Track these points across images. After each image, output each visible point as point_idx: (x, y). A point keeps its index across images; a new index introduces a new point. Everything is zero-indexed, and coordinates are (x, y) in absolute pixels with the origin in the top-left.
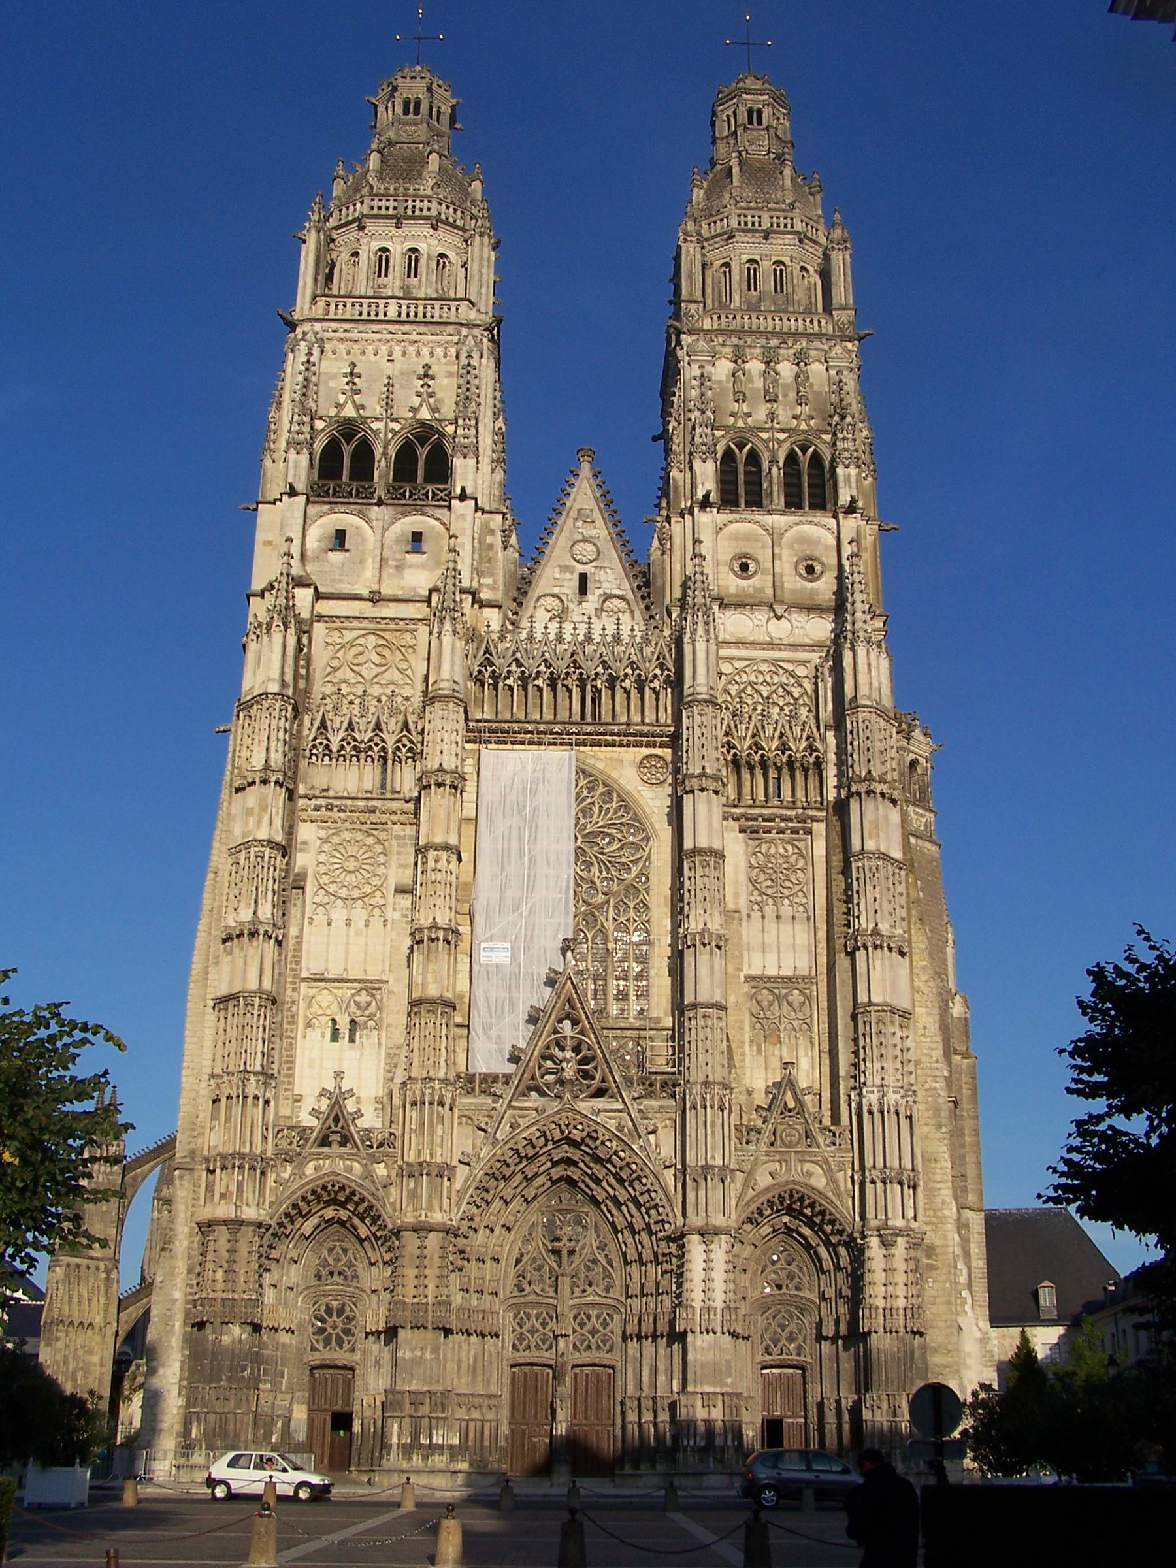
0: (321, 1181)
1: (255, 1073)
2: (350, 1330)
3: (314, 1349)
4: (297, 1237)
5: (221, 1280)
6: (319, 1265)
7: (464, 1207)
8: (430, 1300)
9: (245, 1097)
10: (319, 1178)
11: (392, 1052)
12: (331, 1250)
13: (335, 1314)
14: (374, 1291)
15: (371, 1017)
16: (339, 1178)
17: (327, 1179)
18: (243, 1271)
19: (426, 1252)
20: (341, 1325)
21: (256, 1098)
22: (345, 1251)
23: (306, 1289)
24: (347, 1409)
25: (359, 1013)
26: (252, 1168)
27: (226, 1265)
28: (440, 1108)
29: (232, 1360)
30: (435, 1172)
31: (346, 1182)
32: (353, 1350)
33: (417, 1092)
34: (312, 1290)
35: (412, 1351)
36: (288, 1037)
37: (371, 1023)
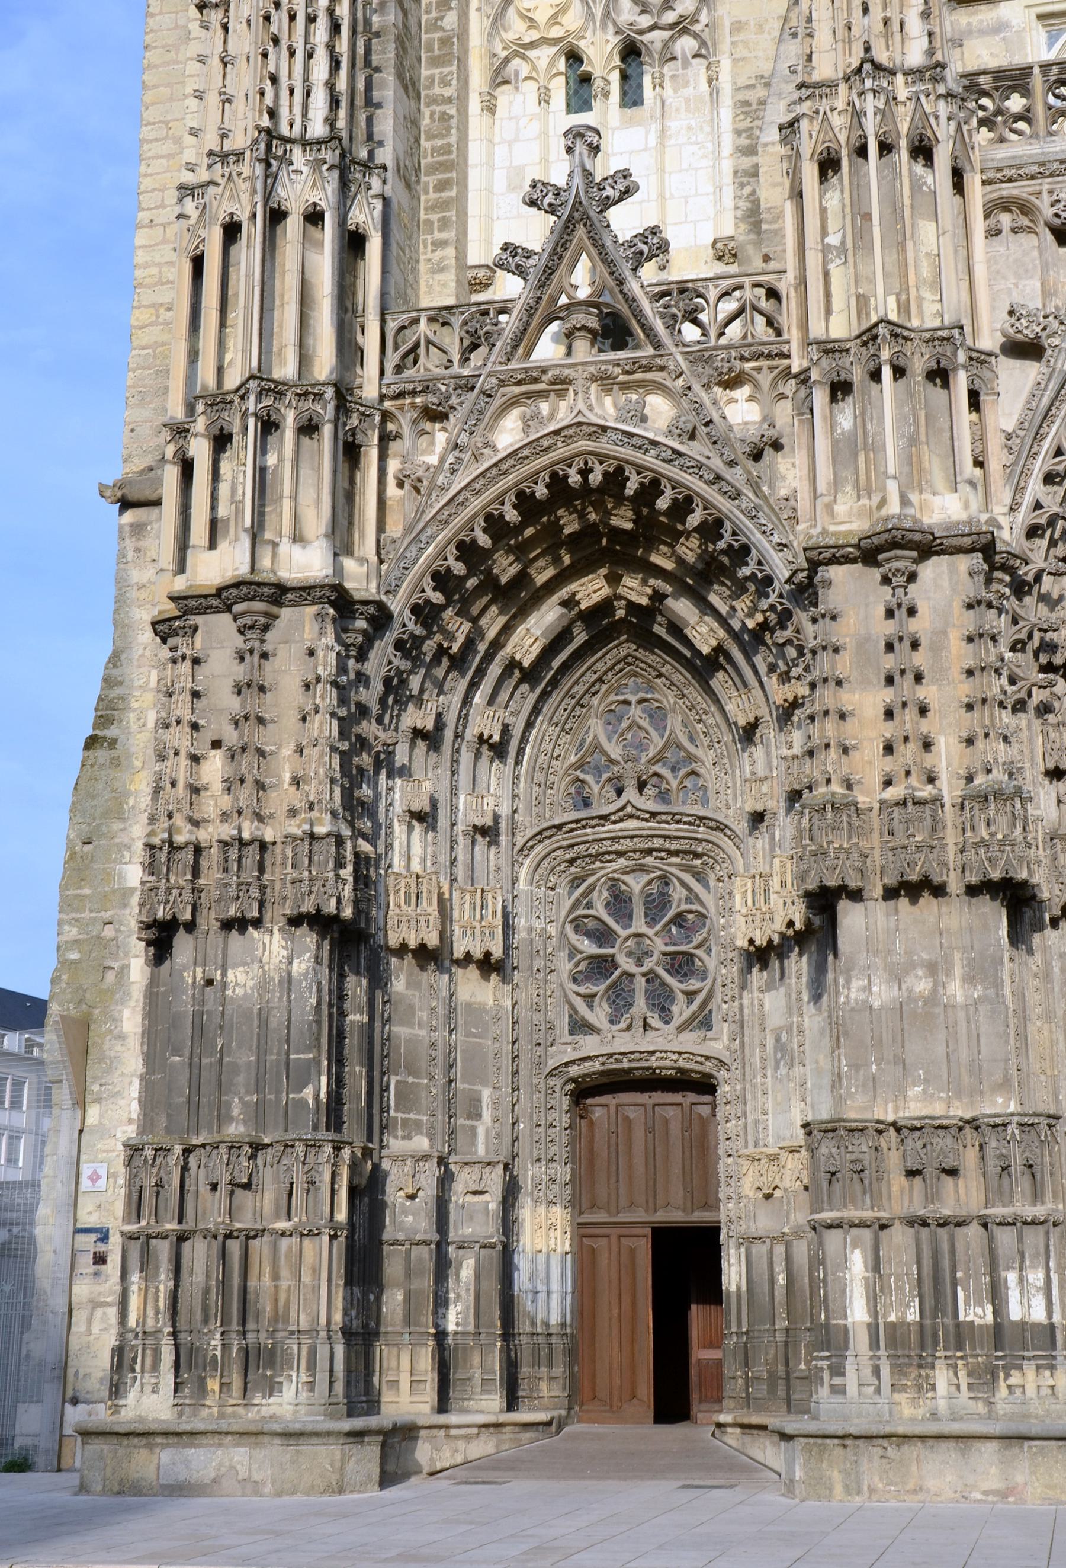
0: (545, 460)
1: (305, 143)
2: (690, 957)
3: (580, 1026)
4: (495, 670)
5: (217, 787)
6: (580, 765)
7: (1035, 488)
8: (949, 789)
9: (276, 216)
10: (535, 447)
11: (752, 96)
12: (612, 717)
13: (638, 910)
14: (757, 818)
15: (681, 27)
16: (603, 445)
17: (562, 451)
18: (288, 751)
19: (914, 625)
20: (660, 946)
21: (314, 217)
22: (658, 716)
23: (540, 836)
24: (700, 1217)
25: (645, 21)
26: (308, 428)
27: (231, 736)
28: (919, 168)
29: (262, 1051)
30: (919, 364)
31: (626, 452)
32: (703, 1021)
33: (838, 121)
34: (560, 839)
35: (897, 976)
36: (434, 101)
37: (686, 44)
